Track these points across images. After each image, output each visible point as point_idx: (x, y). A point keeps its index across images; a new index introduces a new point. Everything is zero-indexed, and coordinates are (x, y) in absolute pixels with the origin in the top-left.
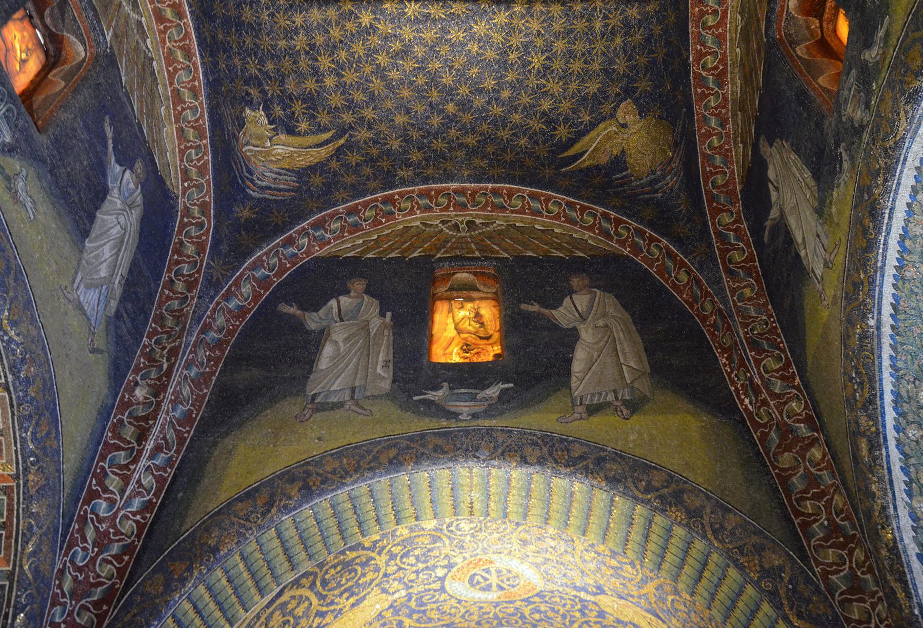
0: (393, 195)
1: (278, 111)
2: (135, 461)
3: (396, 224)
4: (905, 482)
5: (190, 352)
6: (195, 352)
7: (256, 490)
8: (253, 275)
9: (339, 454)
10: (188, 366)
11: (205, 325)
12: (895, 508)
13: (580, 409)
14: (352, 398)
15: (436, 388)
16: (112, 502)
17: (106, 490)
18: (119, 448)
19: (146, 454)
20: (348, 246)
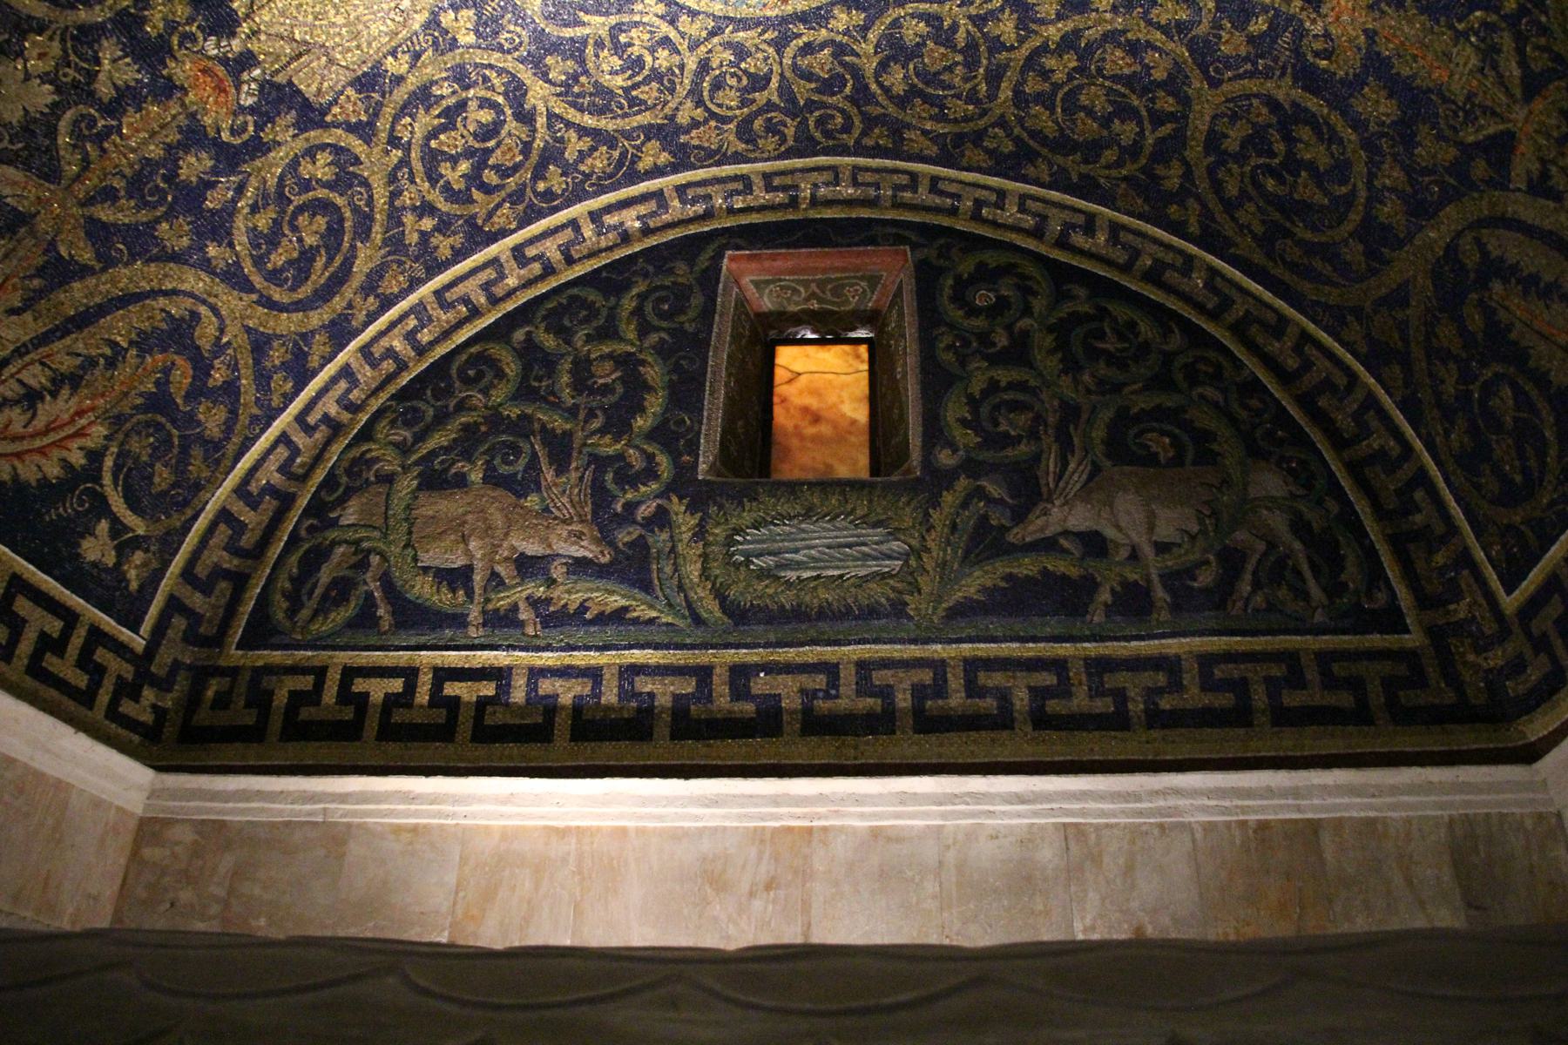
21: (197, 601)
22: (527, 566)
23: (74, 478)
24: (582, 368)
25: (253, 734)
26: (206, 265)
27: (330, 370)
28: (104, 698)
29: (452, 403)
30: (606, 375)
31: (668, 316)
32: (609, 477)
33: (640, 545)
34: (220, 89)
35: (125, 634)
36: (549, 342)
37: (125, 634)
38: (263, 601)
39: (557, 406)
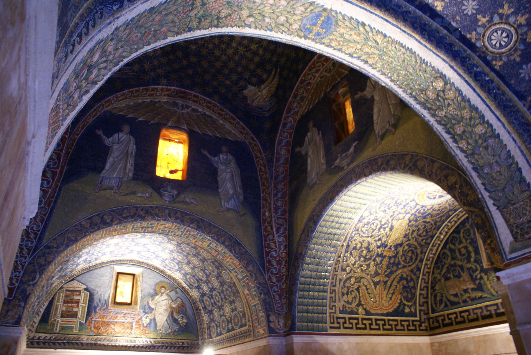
0: (302, 79)
1: (254, 80)
2: (274, 237)
3: (314, 85)
4: (451, 138)
5: (274, 190)
6: (277, 188)
7: (304, 228)
8: (283, 146)
9: (318, 205)
10: (275, 195)
11: (275, 177)
12: (454, 151)
13: (378, 140)
14: (318, 178)
15: (336, 160)
16: (275, 251)
17: (272, 249)
18: (269, 235)
19: (275, 233)
20: (304, 109)
21: (423, 308)
22: (466, 291)
23: (400, 303)
24: (459, 250)
25: (439, 327)
26: (400, 268)
27: (423, 266)
28: (418, 328)
29: (443, 263)
30: (463, 251)
31: (468, 236)
32: (471, 271)
33: (480, 283)
34: (389, 251)
35: (416, 318)
36: (452, 246)
37: (416, 318)
38: (431, 305)
39: (458, 260)
